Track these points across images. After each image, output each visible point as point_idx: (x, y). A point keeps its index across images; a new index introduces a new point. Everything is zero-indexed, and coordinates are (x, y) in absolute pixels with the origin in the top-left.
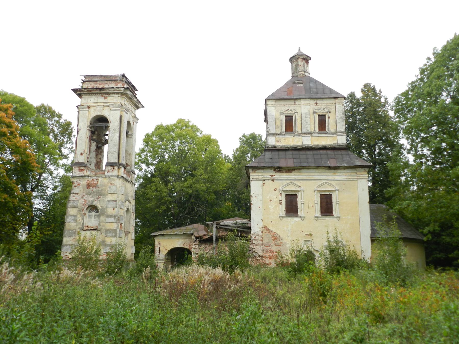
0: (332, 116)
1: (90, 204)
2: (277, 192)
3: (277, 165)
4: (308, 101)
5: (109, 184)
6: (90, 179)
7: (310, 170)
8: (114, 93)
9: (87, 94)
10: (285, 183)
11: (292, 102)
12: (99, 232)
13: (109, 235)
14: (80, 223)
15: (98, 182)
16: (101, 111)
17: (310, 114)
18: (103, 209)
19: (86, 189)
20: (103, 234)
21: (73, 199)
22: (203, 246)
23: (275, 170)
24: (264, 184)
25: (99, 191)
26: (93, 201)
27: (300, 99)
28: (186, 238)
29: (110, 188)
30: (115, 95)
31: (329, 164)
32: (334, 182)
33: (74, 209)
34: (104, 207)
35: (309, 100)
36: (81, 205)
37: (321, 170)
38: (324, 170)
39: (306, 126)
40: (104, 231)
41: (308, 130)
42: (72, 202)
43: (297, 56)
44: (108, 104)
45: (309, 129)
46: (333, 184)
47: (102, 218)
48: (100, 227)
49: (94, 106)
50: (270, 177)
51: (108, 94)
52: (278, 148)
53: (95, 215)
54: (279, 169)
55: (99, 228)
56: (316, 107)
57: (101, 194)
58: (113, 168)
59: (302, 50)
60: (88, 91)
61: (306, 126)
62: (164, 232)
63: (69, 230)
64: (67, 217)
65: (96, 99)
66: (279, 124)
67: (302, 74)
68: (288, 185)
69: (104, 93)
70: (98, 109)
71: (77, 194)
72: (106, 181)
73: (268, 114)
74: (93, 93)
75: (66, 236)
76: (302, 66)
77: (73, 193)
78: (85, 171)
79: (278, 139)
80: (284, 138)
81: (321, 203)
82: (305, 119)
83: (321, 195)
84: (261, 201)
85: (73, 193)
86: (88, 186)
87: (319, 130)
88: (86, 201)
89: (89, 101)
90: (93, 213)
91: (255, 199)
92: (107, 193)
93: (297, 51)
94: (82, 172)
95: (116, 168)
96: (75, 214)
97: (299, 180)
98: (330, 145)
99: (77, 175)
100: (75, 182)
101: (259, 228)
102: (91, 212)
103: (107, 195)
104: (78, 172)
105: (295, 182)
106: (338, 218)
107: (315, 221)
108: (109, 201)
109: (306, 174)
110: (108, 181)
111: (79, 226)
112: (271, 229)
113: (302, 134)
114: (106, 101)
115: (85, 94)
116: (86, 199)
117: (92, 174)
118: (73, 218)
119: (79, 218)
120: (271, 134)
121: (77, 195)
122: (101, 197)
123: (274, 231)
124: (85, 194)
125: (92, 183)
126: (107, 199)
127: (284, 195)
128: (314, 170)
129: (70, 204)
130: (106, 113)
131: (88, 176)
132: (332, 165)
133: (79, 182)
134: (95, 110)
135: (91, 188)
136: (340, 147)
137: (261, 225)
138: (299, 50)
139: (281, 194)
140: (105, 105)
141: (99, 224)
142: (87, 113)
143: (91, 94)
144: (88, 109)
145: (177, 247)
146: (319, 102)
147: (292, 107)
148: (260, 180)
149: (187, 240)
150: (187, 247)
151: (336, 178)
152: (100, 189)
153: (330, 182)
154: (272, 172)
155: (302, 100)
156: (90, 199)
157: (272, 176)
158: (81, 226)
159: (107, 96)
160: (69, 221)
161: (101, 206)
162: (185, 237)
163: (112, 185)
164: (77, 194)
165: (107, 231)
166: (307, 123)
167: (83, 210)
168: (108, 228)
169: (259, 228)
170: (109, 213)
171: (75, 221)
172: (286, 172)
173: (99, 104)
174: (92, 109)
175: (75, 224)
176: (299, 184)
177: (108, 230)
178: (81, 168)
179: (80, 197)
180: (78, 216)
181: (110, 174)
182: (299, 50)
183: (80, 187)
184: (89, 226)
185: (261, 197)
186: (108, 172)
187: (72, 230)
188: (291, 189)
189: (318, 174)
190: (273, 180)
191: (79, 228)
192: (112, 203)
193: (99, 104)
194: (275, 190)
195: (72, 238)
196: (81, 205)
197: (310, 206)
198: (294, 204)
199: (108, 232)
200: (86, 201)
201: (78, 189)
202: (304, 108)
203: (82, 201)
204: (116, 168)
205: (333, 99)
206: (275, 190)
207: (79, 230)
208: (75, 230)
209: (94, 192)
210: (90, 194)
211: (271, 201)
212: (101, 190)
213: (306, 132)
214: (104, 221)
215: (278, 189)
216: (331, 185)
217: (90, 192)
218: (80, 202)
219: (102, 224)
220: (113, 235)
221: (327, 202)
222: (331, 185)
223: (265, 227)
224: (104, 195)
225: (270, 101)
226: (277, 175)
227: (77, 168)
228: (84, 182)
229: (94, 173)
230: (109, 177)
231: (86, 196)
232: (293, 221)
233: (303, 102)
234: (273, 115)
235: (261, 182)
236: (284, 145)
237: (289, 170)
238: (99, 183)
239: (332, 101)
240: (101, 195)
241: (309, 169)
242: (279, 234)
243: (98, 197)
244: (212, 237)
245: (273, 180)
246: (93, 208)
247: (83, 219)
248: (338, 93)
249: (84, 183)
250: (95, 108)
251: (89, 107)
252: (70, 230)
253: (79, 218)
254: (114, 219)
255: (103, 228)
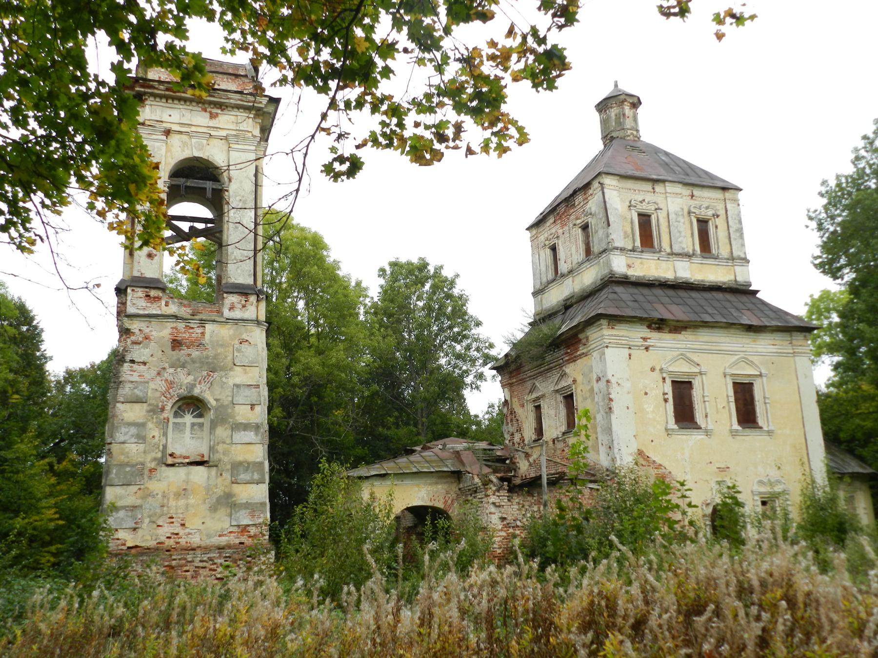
0: (720, 222)
1: (183, 392)
2: (656, 375)
3: (656, 315)
4: (678, 189)
5: (237, 342)
6: (181, 325)
7: (716, 330)
8: (238, 107)
9: (161, 97)
10: (670, 355)
11: (648, 186)
12: (214, 470)
13: (243, 476)
14: (156, 446)
15: (203, 334)
16: (201, 148)
17: (683, 215)
18: (222, 406)
19: (169, 350)
20: (227, 476)
21: (132, 379)
22: (516, 499)
23: (649, 327)
24: (630, 355)
25: (207, 357)
26: (192, 386)
27: (663, 181)
28: (437, 483)
29: (239, 351)
30: (242, 114)
31: (745, 321)
32: (756, 358)
33: (137, 406)
34: (226, 403)
35: (680, 186)
36: (158, 394)
37: (732, 331)
38: (737, 332)
39: (680, 240)
40: (229, 467)
41: (683, 249)
42: (128, 385)
43: (623, 97)
44: (224, 133)
45: (684, 246)
46: (756, 362)
47: (221, 432)
48: (216, 457)
49: (181, 132)
50: (641, 342)
51: (221, 106)
52: (633, 279)
53: (193, 425)
54: (659, 325)
55: (215, 457)
56: (693, 203)
57: (213, 367)
58: (243, 299)
59: (620, 87)
60: (167, 89)
61: (680, 240)
62: (388, 466)
63: (122, 465)
64: (114, 428)
65: (188, 114)
66: (629, 230)
67: (632, 134)
68: (675, 360)
69: (210, 103)
70: (194, 140)
71: (144, 363)
72: (226, 332)
73: (608, 206)
74: (180, 99)
75: (116, 482)
76: (631, 119)
77: (133, 361)
78: (163, 303)
79: (630, 261)
80: (640, 261)
81: (737, 400)
82: (676, 224)
83: (734, 383)
84: (629, 393)
85: (133, 361)
86: (176, 344)
87: (701, 251)
88: (170, 384)
89: (165, 118)
90: (188, 419)
91: (617, 389)
92: (230, 365)
93: (612, 88)
94: (155, 305)
95: (253, 299)
96: (141, 421)
97: (695, 351)
98: (724, 283)
99: (141, 312)
100: (137, 331)
101: (631, 454)
102: (182, 417)
103: (231, 369)
104: (143, 303)
105: (688, 355)
106: (770, 433)
107: (730, 438)
108: (238, 386)
109: (706, 338)
110: (231, 332)
111: (153, 455)
112: (654, 457)
113: (672, 254)
114: (212, 123)
115: (155, 96)
116: (170, 378)
117: (184, 312)
118: (133, 430)
119: (153, 431)
120: (617, 248)
121: (142, 367)
122: (216, 375)
123: (658, 461)
124: (166, 365)
125: (187, 335)
126: (231, 382)
127: (668, 382)
128: (721, 331)
129: (125, 391)
130: (216, 154)
131: (176, 317)
132: (755, 322)
133: (147, 330)
134: (185, 144)
135: (185, 351)
136: (742, 287)
137: (634, 449)
138: (616, 85)
139: (664, 379)
140: (213, 133)
141: (212, 449)
142: (164, 148)
143: (173, 99)
144: (164, 138)
145: (415, 504)
146: (697, 192)
147: (649, 197)
148: (622, 346)
149: (440, 486)
150: (440, 505)
151: (759, 350)
152: (211, 353)
153: (750, 358)
154: (643, 331)
155: (667, 184)
156: (184, 379)
157: (645, 339)
158: (159, 455)
159: (219, 111)
160: (122, 439)
161: (217, 400)
162: (434, 480)
163: (244, 346)
164: (144, 363)
165: (236, 466)
166: (680, 232)
167: (163, 409)
168: (240, 458)
169: (631, 454)
170: (240, 419)
171: (141, 438)
172: (670, 332)
173: (194, 129)
174: (175, 139)
175: (141, 447)
176: (695, 357)
177: (240, 464)
178: (153, 293)
179: (153, 373)
180: (150, 425)
181: (237, 314)
182: (616, 85)
183: (152, 344)
184: (178, 452)
185: (627, 385)
186: (232, 308)
187: (133, 466)
188: (682, 369)
189: (728, 339)
190: (647, 349)
191: (155, 459)
192: (247, 392)
193: (194, 129)
194: (653, 369)
195: (134, 489)
196: (158, 394)
197: (720, 406)
198: (687, 403)
199: (241, 469)
200: (170, 384)
201: (147, 352)
202: (673, 202)
203: (158, 384)
204: (253, 299)
205: (720, 191)
206: (653, 369)
207: (153, 465)
208: (143, 464)
209: (194, 362)
210: (183, 366)
211: (646, 394)
212: (216, 357)
213: (680, 252)
214: (228, 441)
215: (658, 368)
216: (751, 364)
217: (182, 359)
218: (152, 385)
219: (220, 448)
220: (256, 476)
221: (745, 400)
222: (751, 364)
223: (640, 453)
224: (223, 369)
225: (610, 177)
226: (656, 338)
227: (140, 292)
228: (163, 332)
229: (189, 310)
230: (236, 321)
231: (171, 370)
232: (691, 439)
233: (670, 188)
234: (616, 209)
235: (627, 351)
236: (641, 274)
237: (678, 327)
238: (207, 336)
239: (718, 194)
240: (213, 371)
241: (713, 327)
242: (669, 469)
243: (205, 373)
244: (539, 478)
245: (647, 349)
246: (188, 404)
247: (165, 434)
248: (724, 181)
249: (162, 334)
250: (184, 137)
251: (168, 132)
252: (127, 464)
253: (153, 431)
254: (257, 434)
255: (226, 459)
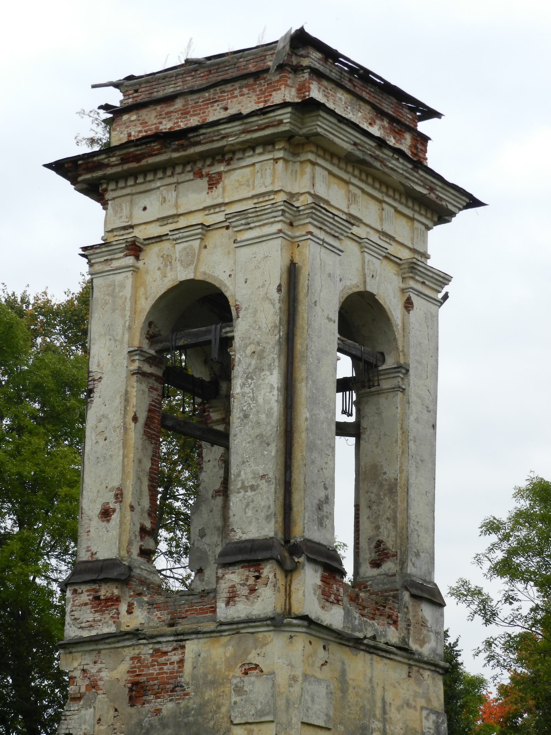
5: (238, 672)
6: (146, 651)
15: (181, 662)
29: (239, 690)
49: (159, 238)
60: (124, 160)
65: (171, 195)
69: (203, 156)
70: (179, 247)
74: (155, 169)
78: (123, 608)
89: (139, 217)
92: (225, 724)
99: (85, 634)
100: (77, 674)
104: (87, 615)
110: (230, 650)
115: (115, 178)
125: (154, 671)
134: (167, 260)
135: (153, 703)
142: (129, 283)
143: (145, 171)
144: (130, 260)
152: (192, 702)
159: (222, 168)
163: (252, 677)
173: (183, 222)
178: (105, 591)
186: (231, 600)
193: (183, 222)
238: (188, 667)
249: (116, 674)
250: (166, 245)
